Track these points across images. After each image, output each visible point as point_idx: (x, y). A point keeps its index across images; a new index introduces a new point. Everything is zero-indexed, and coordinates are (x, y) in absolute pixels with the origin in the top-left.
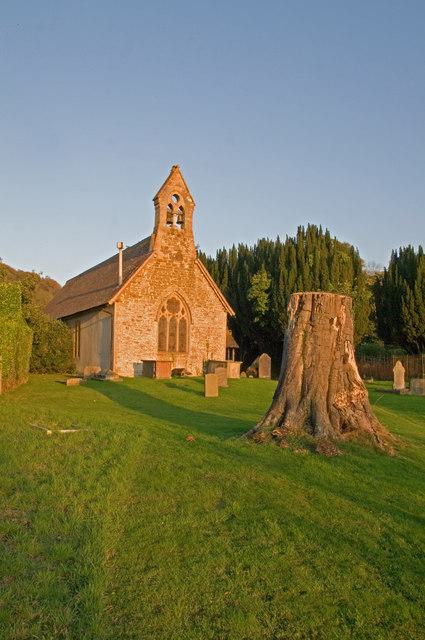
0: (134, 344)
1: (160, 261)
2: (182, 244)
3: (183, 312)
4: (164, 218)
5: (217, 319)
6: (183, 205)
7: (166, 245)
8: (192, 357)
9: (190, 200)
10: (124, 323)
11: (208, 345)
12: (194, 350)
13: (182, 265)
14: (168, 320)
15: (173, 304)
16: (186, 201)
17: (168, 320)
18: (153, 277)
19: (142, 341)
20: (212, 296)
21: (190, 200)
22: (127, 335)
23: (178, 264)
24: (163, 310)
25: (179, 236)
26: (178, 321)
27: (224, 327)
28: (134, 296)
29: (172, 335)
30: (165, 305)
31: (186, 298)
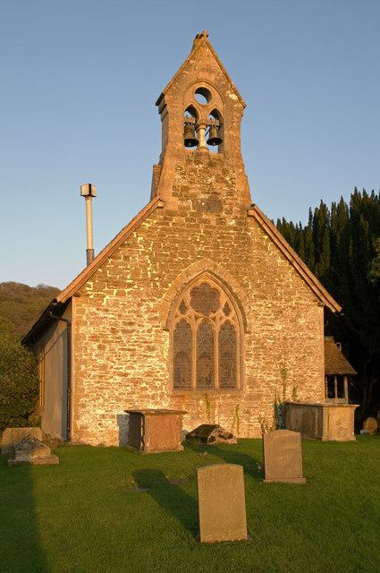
0: (119, 379)
1: (171, 214)
2: (220, 180)
3: (227, 311)
4: (178, 134)
5: (302, 321)
6: (220, 108)
7: (184, 183)
8: (250, 398)
9: (234, 97)
10: (94, 338)
11: (284, 373)
12: (253, 382)
13: (221, 221)
14: (195, 327)
15: (204, 298)
16: (225, 99)
17: (195, 327)
18: (157, 246)
19: (137, 371)
20: (290, 277)
21: (234, 97)
22: (101, 362)
23: (212, 218)
24: (183, 308)
25: (211, 165)
26: (217, 328)
27: (319, 335)
28: (116, 284)
29: (205, 356)
30: (188, 297)
31: (233, 282)
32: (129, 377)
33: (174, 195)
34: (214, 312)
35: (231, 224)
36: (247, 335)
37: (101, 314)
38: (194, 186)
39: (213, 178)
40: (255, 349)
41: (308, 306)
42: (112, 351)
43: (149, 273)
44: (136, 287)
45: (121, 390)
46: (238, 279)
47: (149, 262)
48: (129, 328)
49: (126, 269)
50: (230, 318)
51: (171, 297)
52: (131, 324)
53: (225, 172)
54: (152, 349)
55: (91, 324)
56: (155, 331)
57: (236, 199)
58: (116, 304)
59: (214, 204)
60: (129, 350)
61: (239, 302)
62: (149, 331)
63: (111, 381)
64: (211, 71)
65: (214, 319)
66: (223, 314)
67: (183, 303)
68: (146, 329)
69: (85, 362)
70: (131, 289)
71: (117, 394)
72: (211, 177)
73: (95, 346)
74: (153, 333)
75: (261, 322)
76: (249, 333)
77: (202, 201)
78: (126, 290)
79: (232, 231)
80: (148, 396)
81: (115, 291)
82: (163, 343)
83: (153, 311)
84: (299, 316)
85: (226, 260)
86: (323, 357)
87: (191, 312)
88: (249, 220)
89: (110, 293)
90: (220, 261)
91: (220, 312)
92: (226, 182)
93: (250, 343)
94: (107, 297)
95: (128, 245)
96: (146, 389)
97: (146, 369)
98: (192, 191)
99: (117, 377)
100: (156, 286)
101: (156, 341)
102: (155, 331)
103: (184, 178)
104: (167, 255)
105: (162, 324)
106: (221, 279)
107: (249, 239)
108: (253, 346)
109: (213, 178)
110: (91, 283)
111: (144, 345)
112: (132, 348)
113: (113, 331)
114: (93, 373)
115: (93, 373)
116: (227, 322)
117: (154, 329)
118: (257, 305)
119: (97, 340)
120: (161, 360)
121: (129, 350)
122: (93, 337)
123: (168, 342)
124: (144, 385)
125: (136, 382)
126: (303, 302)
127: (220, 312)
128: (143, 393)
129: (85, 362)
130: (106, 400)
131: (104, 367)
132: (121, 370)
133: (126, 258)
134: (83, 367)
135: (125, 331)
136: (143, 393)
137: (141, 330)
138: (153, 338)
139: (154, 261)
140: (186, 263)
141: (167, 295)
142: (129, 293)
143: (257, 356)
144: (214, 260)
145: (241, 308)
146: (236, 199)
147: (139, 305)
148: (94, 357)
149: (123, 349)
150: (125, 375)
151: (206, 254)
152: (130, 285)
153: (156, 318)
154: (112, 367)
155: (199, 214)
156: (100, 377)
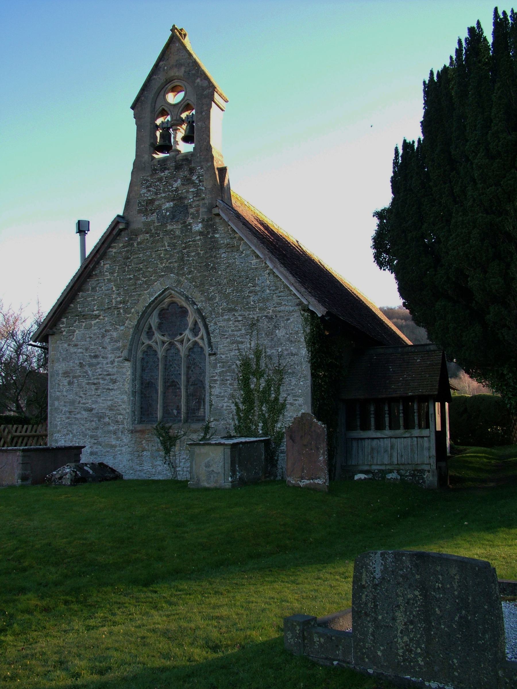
0: (85, 414)
1: (136, 233)
2: (188, 181)
3: (195, 331)
5: (280, 333)
7: (149, 196)
10: (66, 374)
13: (186, 228)
17: (161, 352)
19: (101, 405)
22: (71, 397)
23: (175, 227)
25: (178, 167)
26: (183, 350)
29: (171, 385)
30: (154, 321)
31: (198, 297)
32: (94, 412)
33: (140, 212)
34: (181, 334)
35: (197, 229)
36: (213, 358)
37: (72, 350)
38: (159, 196)
39: (179, 181)
40: (221, 374)
41: (290, 312)
42: (80, 386)
43: (114, 301)
44: (101, 317)
45: (88, 425)
46: (202, 292)
47: (114, 289)
48: (94, 361)
49: (93, 300)
50: (197, 339)
51: (135, 322)
52: (96, 357)
53: (192, 171)
54: (114, 382)
55: (63, 360)
56: (118, 362)
57: (203, 199)
58: (84, 338)
59: (181, 209)
60: (94, 384)
61: (204, 319)
62: (112, 362)
63: (78, 416)
64: (179, 65)
65: (182, 342)
66: (190, 337)
67: (150, 328)
68: (109, 360)
69: (58, 399)
70: (97, 320)
71: (84, 430)
72: (176, 181)
73: (66, 382)
74: (116, 364)
75: (228, 340)
76: (215, 354)
77: (167, 210)
78: (93, 322)
79: (198, 238)
80: (109, 432)
81: (84, 324)
82: (125, 374)
83: (116, 341)
84: (276, 327)
85: (190, 272)
86: (309, 377)
87: (157, 336)
88: (217, 220)
89: (79, 327)
90: (183, 274)
91: (187, 333)
92: (193, 183)
93: (215, 367)
94: (77, 332)
95: (96, 275)
96: (109, 424)
97: (109, 403)
98: (157, 203)
99: (83, 412)
100: (119, 314)
101: (118, 372)
102: (118, 362)
103: (149, 191)
104: (131, 279)
105: (125, 353)
106: (183, 295)
107: (217, 242)
108: (218, 370)
109: (179, 181)
110: (64, 320)
111: (108, 378)
112: (96, 381)
113: (81, 365)
114: (65, 409)
115: (65, 409)
116: (196, 343)
117: (116, 360)
118: (224, 320)
119: (68, 376)
120: (121, 394)
121: (94, 384)
122: (64, 373)
123: (129, 373)
124: (107, 420)
125: (100, 417)
126: (282, 308)
127: (187, 333)
128: (106, 429)
129: (58, 399)
130: (74, 436)
131: (72, 403)
132: (87, 405)
133: (94, 289)
134: (56, 403)
135: (91, 365)
136: (106, 429)
137: (105, 362)
138: (115, 370)
139: (118, 287)
140: (149, 284)
141: (131, 323)
142: (95, 324)
143: (223, 382)
144: (178, 274)
145: (206, 326)
146: (203, 199)
147: (103, 336)
148: (65, 394)
149: (88, 384)
150: (91, 410)
151: (169, 270)
152: (97, 317)
153: (118, 348)
154: (79, 402)
155: (164, 225)
156: (70, 412)
